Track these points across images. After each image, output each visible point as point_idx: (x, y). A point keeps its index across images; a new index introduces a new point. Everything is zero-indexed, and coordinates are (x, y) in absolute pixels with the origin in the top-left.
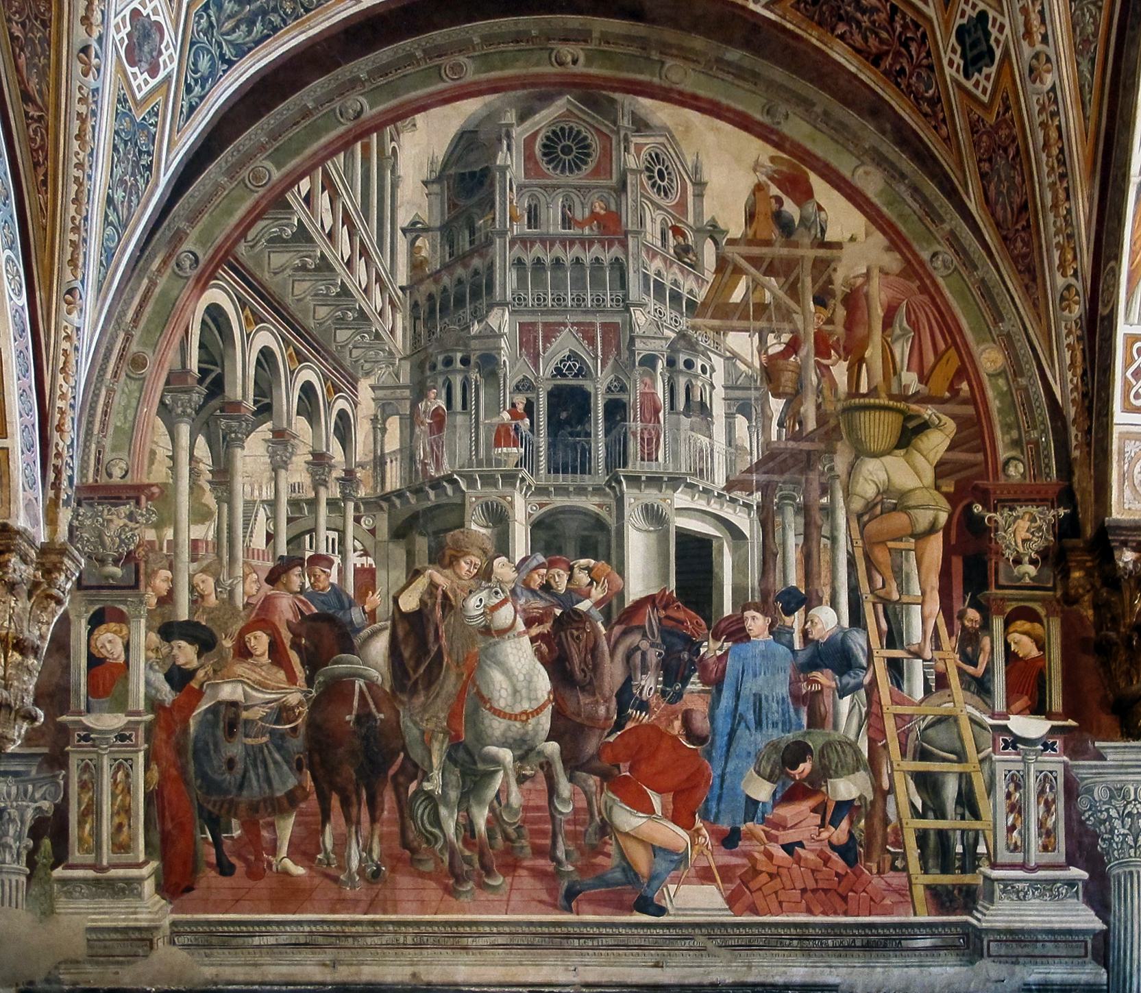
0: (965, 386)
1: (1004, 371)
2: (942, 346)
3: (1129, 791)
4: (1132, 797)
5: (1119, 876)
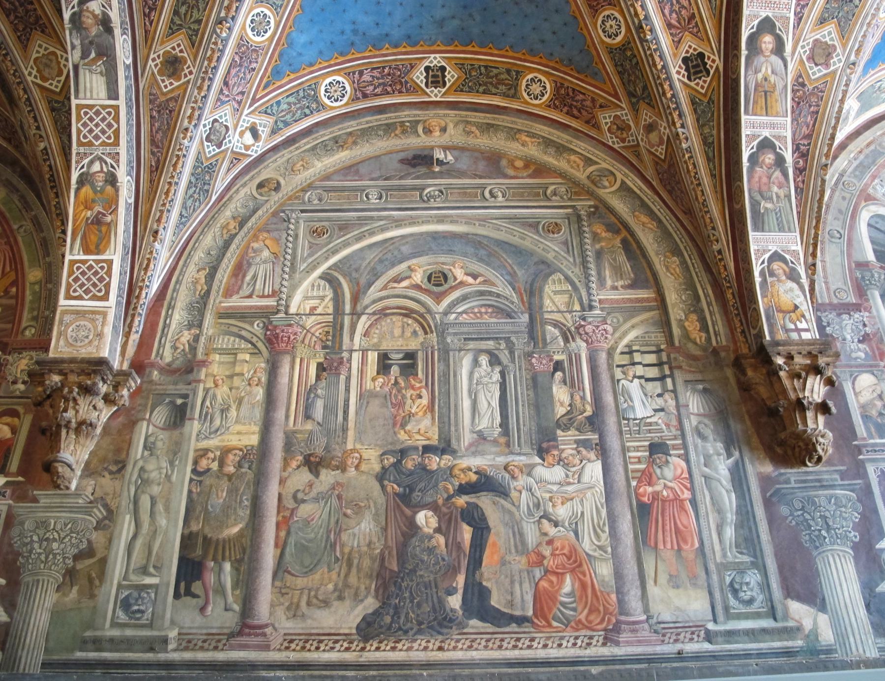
0: (14, 290)
1: (41, 281)
2: (8, 269)
3: (50, 524)
4: (52, 527)
5: (28, 582)
